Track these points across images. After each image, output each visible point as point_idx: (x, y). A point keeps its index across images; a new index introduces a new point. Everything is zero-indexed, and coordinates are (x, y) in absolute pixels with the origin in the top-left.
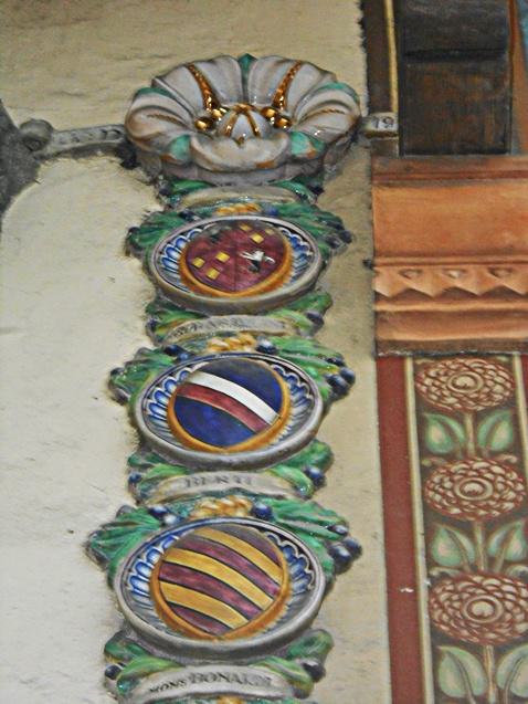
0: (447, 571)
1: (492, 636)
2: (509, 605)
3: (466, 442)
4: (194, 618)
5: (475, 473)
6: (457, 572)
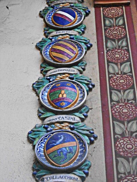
0: (110, 49)
1: (119, 61)
3: (113, 24)
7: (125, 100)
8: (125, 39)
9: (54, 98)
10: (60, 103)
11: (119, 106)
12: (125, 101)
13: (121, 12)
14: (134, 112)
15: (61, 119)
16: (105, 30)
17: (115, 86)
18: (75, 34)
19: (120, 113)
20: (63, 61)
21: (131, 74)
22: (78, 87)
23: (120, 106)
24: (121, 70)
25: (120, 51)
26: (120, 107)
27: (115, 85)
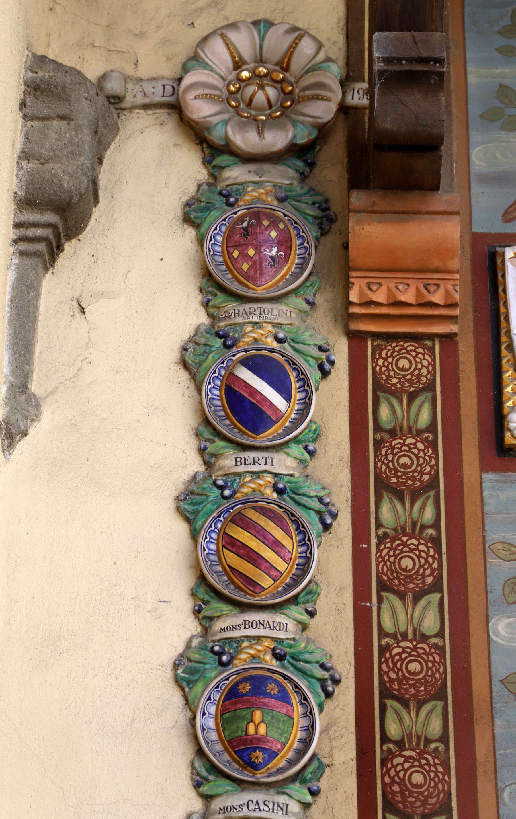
0: (388, 531)
1: (412, 586)
2: (422, 561)
4: (244, 579)
5: (406, 448)
6: (393, 532)
7: (419, 738)
8: (432, 493)
9: (234, 732)
10: (249, 752)
11: (402, 760)
12: (418, 744)
13: (427, 368)
14: (440, 786)
15: (253, 808)
16: (378, 445)
17: (396, 683)
18: (291, 472)
19: (405, 785)
20: (257, 590)
21: (440, 644)
22: (295, 692)
23: (407, 759)
24: (415, 626)
25: (415, 542)
26: (405, 762)
27: (395, 680)
